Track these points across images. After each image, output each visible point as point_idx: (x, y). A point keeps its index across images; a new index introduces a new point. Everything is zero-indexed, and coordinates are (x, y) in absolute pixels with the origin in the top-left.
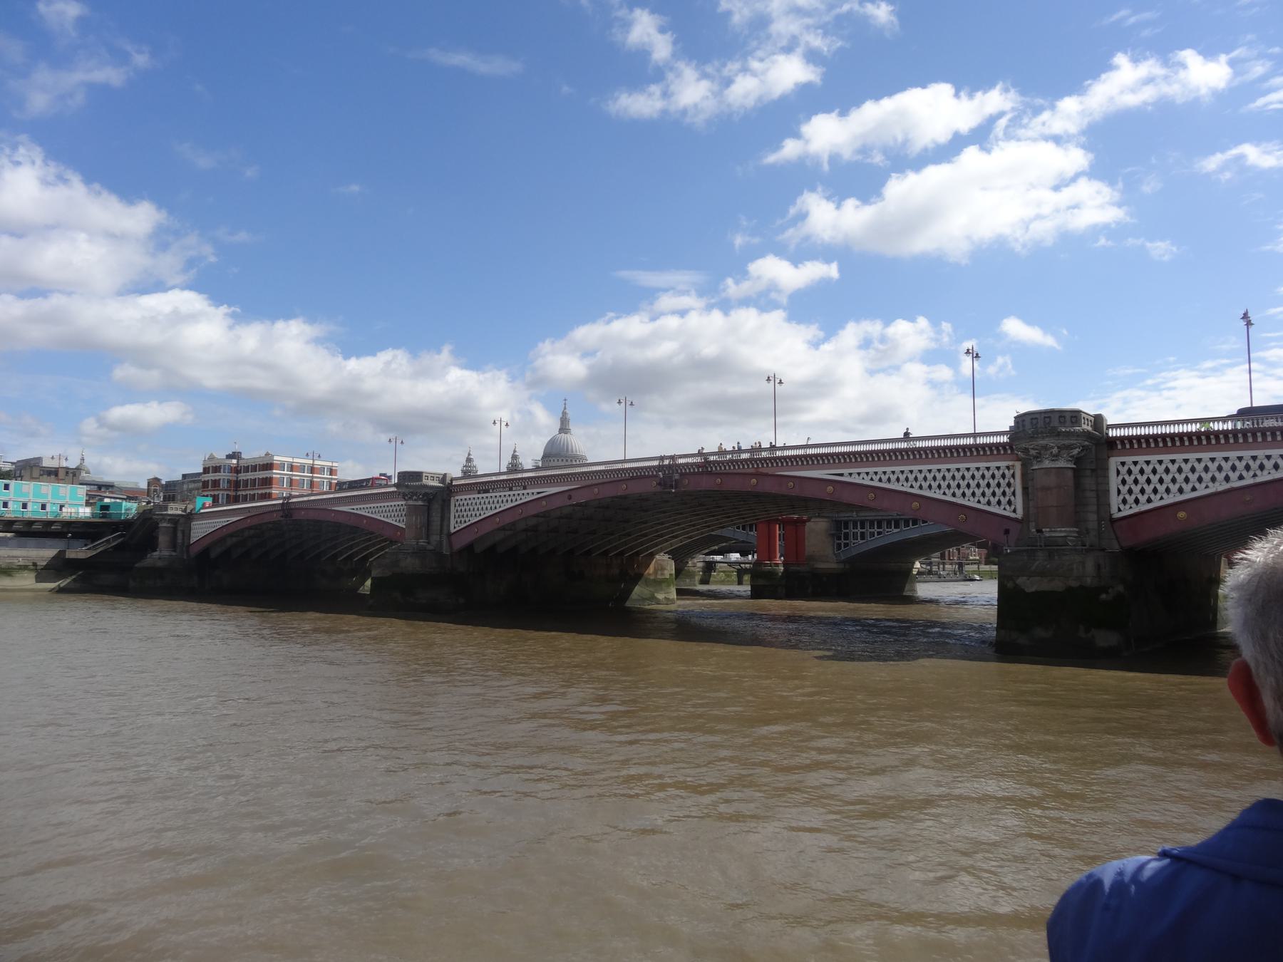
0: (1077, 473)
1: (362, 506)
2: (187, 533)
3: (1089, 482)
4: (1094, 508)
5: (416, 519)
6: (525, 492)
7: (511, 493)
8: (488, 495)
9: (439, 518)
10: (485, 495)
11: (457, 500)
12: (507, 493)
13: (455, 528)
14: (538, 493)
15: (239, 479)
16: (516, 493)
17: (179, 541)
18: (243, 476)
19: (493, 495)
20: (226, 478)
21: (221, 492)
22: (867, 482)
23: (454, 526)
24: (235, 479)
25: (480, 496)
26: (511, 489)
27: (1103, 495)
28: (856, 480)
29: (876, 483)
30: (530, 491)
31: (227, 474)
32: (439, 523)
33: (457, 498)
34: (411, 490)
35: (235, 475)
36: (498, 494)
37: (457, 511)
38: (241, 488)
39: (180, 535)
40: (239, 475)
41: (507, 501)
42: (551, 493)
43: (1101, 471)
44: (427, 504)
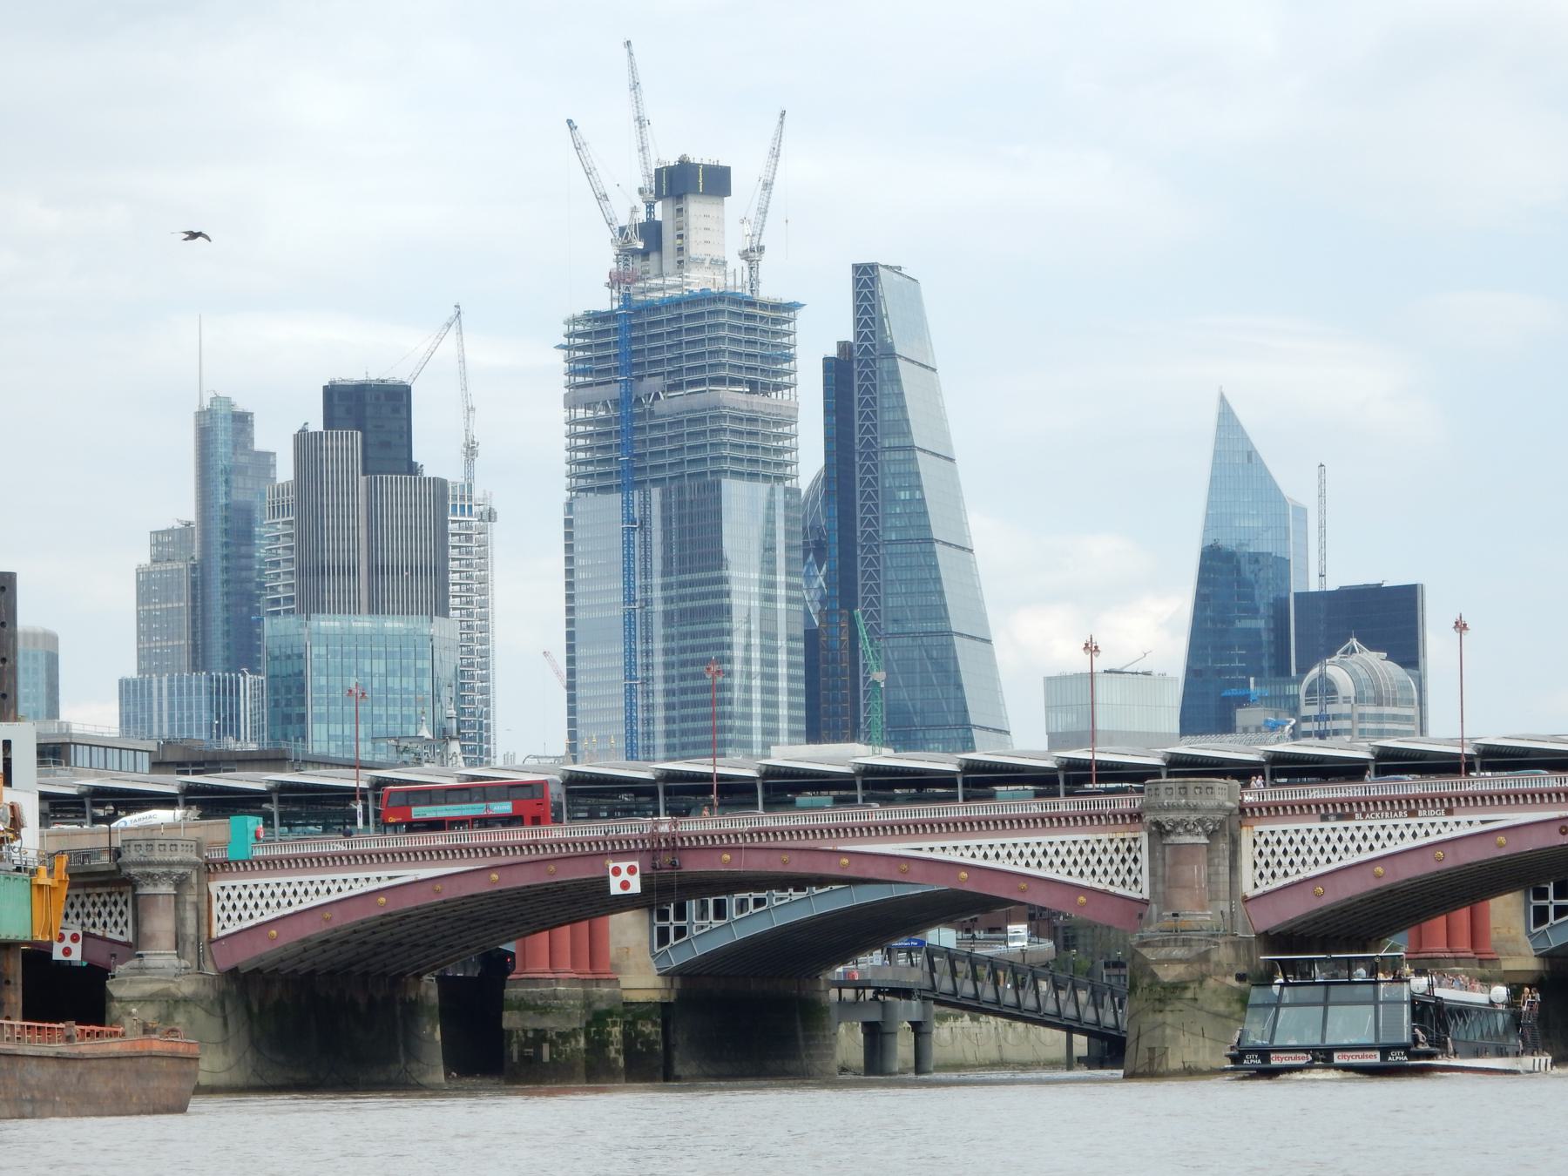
1: (949, 844)
5: (1199, 870)
6: (1451, 819)
7: (1414, 821)
8: (1351, 824)
9: (1227, 870)
10: (1340, 825)
11: (1261, 833)
12: (1402, 822)
13: (1256, 886)
14: (1483, 822)
16: (1426, 821)
17: (190, 929)
19: (1364, 824)
25: (1327, 825)
30: (1463, 819)
32: (1227, 878)
33: (1257, 828)
34: (1200, 816)
36: (1377, 823)
37: (1261, 854)
41: (1402, 836)
42: (1517, 822)
44: (1208, 842)
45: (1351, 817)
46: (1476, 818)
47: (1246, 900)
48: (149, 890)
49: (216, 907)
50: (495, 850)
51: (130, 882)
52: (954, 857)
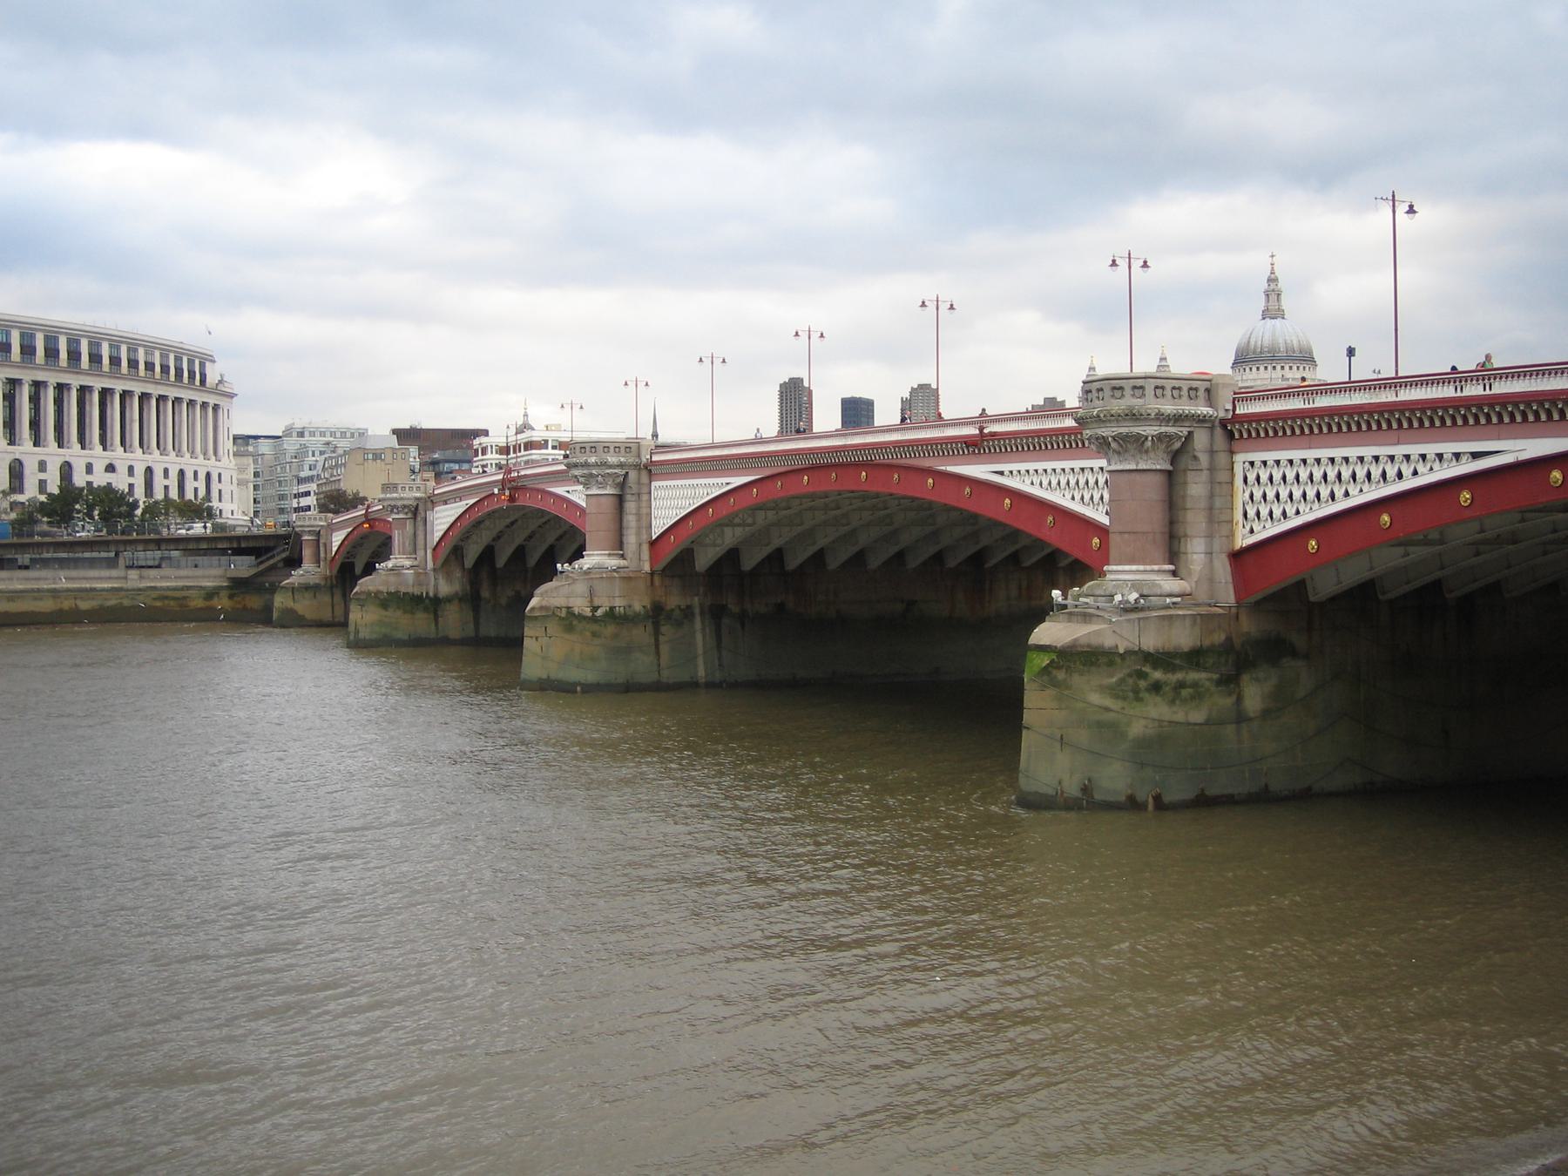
0: (620, 499)
3: (630, 506)
20: (494, 462)
27: (645, 520)
39: (322, 549)
43: (644, 495)
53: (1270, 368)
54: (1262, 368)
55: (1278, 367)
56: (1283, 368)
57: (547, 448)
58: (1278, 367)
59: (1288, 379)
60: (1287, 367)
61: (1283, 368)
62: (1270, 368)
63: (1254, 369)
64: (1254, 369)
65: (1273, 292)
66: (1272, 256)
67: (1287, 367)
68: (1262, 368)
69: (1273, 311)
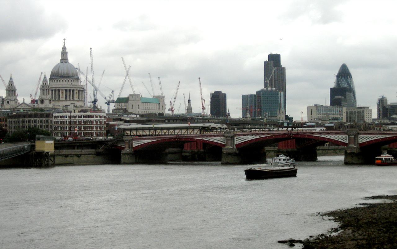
0: (355, 138)
2: (132, 144)
3: (356, 139)
4: (356, 142)
6: (256, 136)
12: (251, 136)
15: (71, 120)
17: (130, 146)
18: (73, 119)
20: (67, 120)
21: (66, 126)
22: (326, 137)
23: (236, 143)
24: (69, 120)
26: (252, 136)
27: (358, 141)
28: (324, 137)
29: (327, 137)
31: (68, 119)
35: (70, 119)
38: (73, 124)
39: (130, 145)
40: (71, 119)
43: (358, 137)
45: (246, 136)
46: (259, 136)
47: (236, 145)
48: (125, 142)
49: (133, 144)
50: (161, 138)
51: (124, 141)
52: (206, 140)
53: (67, 81)
54: (64, 81)
55: (70, 81)
56: (71, 81)
57: (82, 118)
58: (70, 81)
59: (74, 85)
60: (73, 81)
61: (71, 81)
62: (67, 81)
63: (61, 81)
64: (61, 81)
65: (64, 53)
66: (64, 40)
67: (73, 81)
68: (64, 81)
69: (64, 59)
